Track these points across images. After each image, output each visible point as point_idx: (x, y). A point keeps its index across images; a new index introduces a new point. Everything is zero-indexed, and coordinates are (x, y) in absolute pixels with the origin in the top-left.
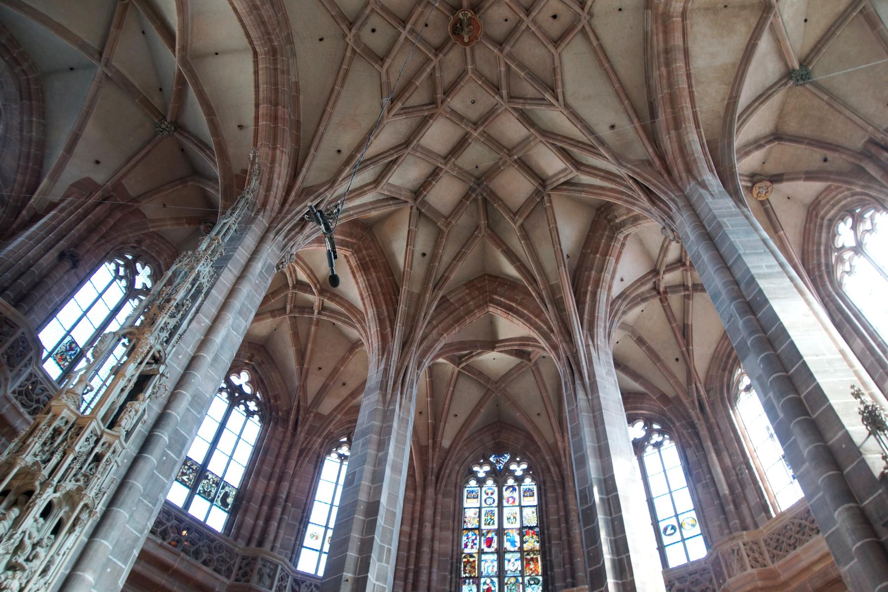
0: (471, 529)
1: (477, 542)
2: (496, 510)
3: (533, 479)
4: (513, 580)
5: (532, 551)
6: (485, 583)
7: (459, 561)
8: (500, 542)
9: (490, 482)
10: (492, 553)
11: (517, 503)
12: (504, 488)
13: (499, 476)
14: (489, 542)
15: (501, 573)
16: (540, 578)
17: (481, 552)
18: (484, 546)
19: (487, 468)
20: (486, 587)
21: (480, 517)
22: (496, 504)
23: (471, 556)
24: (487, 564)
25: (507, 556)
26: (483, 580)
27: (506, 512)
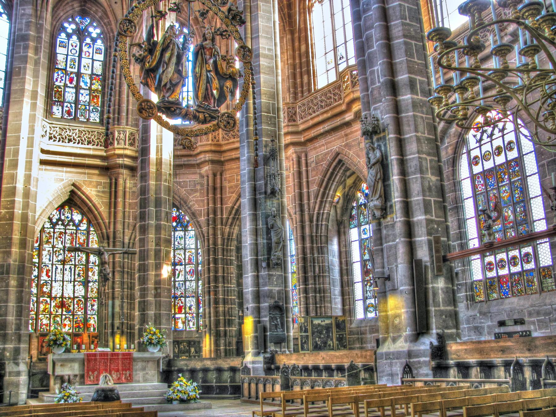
0: (61, 69)
1: (64, 78)
2: (77, 58)
3: (103, 42)
4: (83, 107)
5: (96, 90)
6: (67, 106)
7: (52, 90)
8: (78, 82)
9: (75, 38)
10: (72, 87)
11: (91, 57)
12: (84, 44)
13: (81, 34)
14: (71, 80)
15: (77, 101)
16: (99, 109)
17: (66, 86)
18: (68, 82)
19: (73, 26)
20: (67, 109)
21: (66, 61)
22: (77, 55)
23: (59, 87)
24: (69, 95)
25: (82, 91)
26: (65, 104)
27: (84, 61)
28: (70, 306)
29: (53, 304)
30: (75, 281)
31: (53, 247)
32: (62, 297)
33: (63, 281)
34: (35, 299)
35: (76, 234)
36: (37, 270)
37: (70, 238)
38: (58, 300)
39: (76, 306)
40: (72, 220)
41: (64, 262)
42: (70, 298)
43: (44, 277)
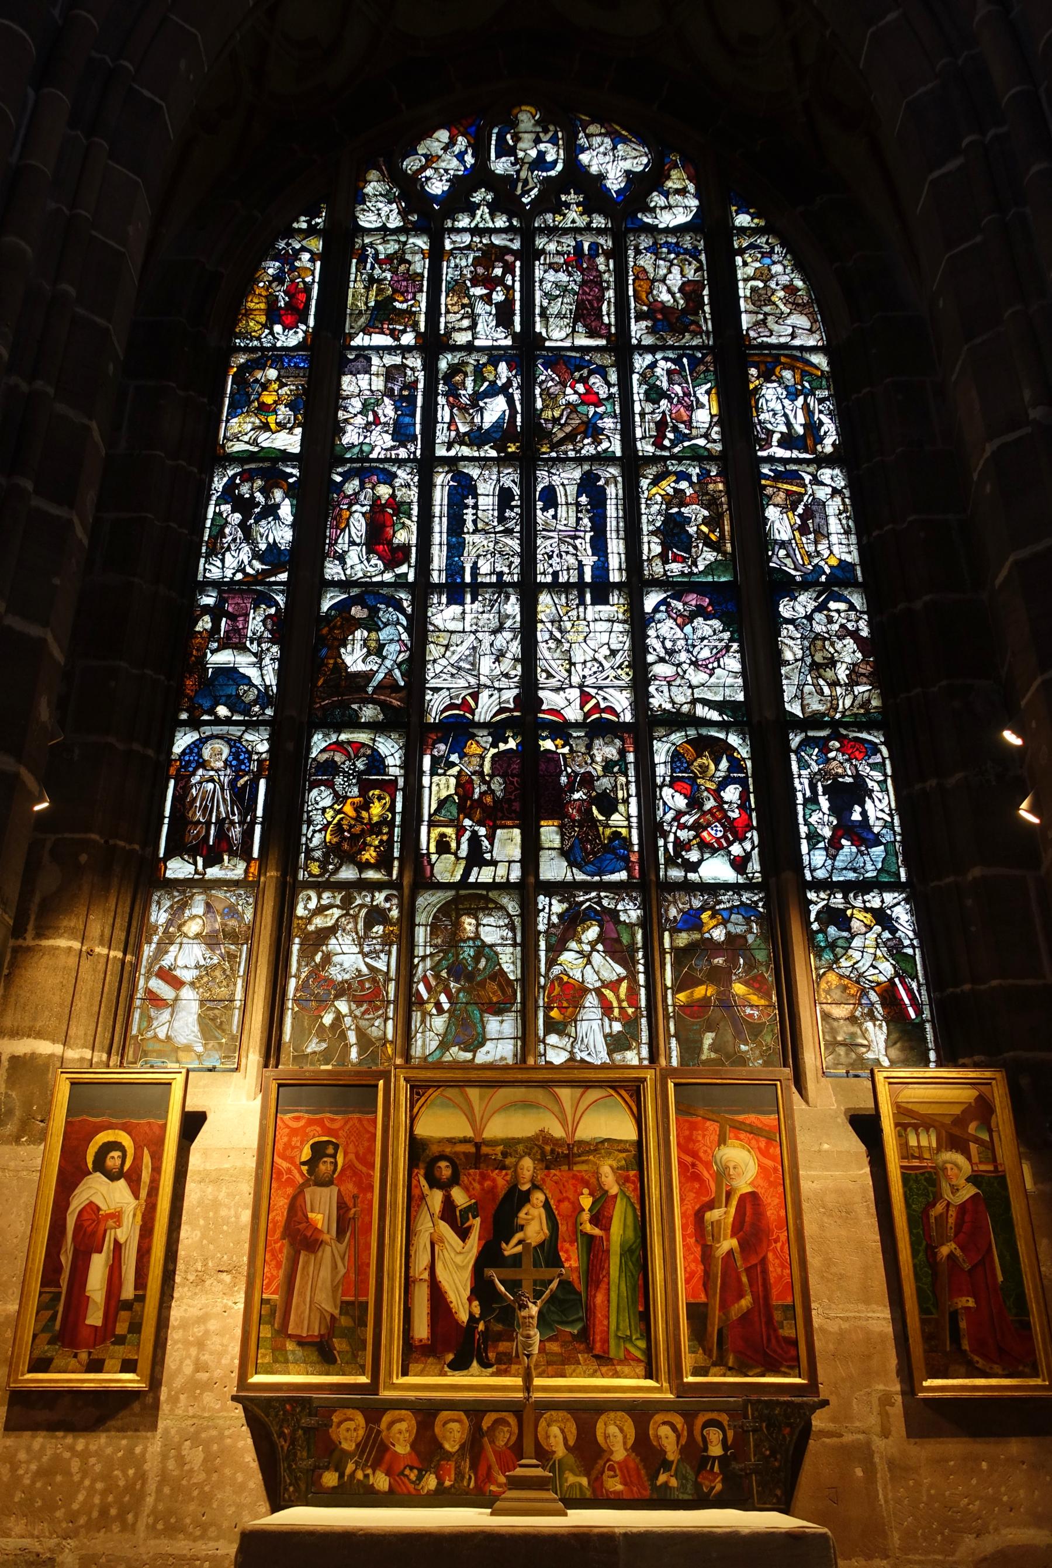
28: (608, 804)
29: (438, 788)
30: (636, 584)
31: (433, 344)
32: (526, 714)
33: (528, 590)
34: (259, 743)
35: (618, 254)
36: (286, 511)
37: (571, 280)
38: (483, 751)
39: (674, 799)
40: (577, 178)
41: (524, 444)
42: (600, 727)
43: (354, 561)
